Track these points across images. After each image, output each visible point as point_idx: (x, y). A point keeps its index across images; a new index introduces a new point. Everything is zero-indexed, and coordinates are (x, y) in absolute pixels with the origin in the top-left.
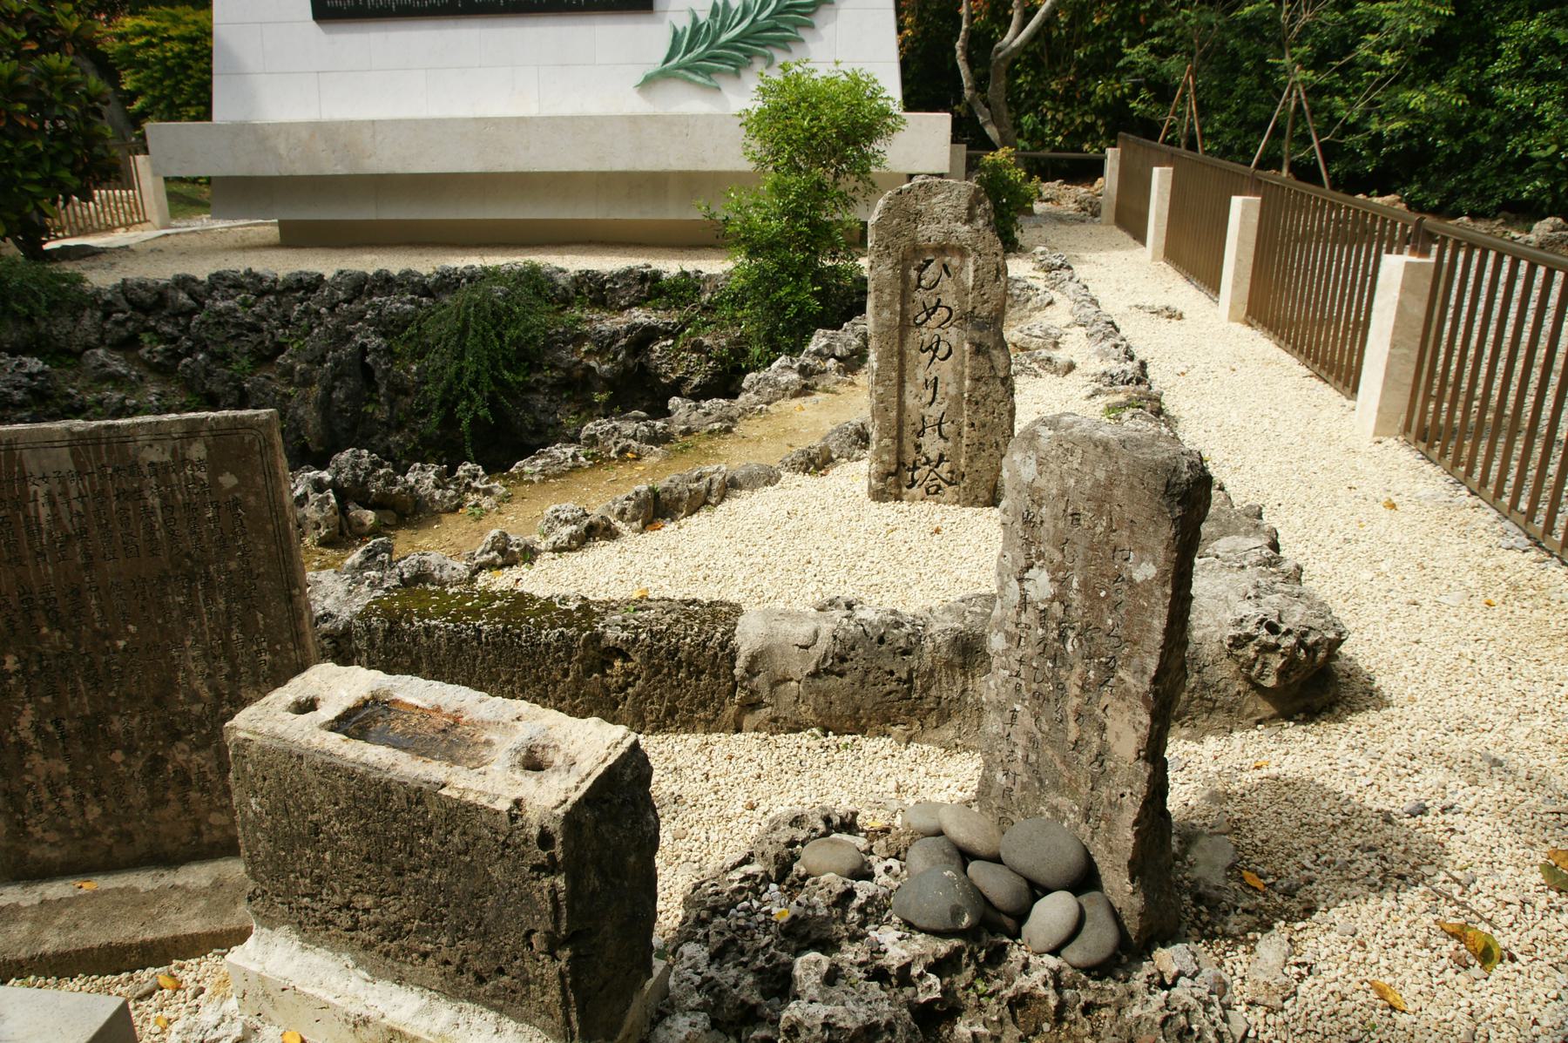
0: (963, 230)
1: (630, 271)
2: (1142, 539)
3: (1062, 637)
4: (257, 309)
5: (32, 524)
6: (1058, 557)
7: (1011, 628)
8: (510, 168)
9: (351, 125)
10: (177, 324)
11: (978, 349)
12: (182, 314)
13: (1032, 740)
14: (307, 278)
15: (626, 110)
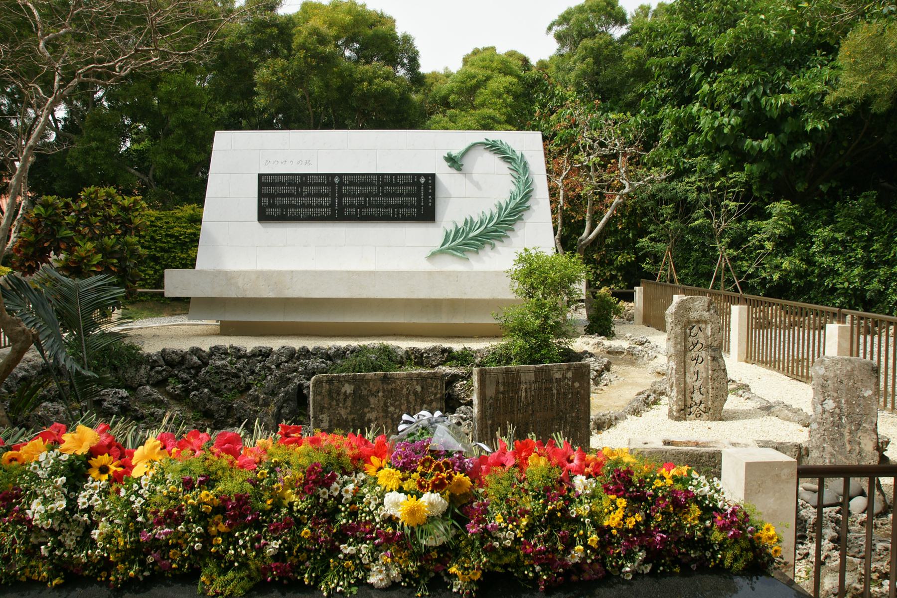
0: (706, 314)
1: (435, 348)
2: (866, 384)
3: (840, 419)
4: (238, 366)
5: (519, 398)
6: (836, 395)
7: (819, 420)
8: (364, 296)
9: (280, 273)
10: (189, 373)
11: (714, 359)
12: (193, 368)
13: (832, 455)
14: (264, 350)
15: (421, 269)
